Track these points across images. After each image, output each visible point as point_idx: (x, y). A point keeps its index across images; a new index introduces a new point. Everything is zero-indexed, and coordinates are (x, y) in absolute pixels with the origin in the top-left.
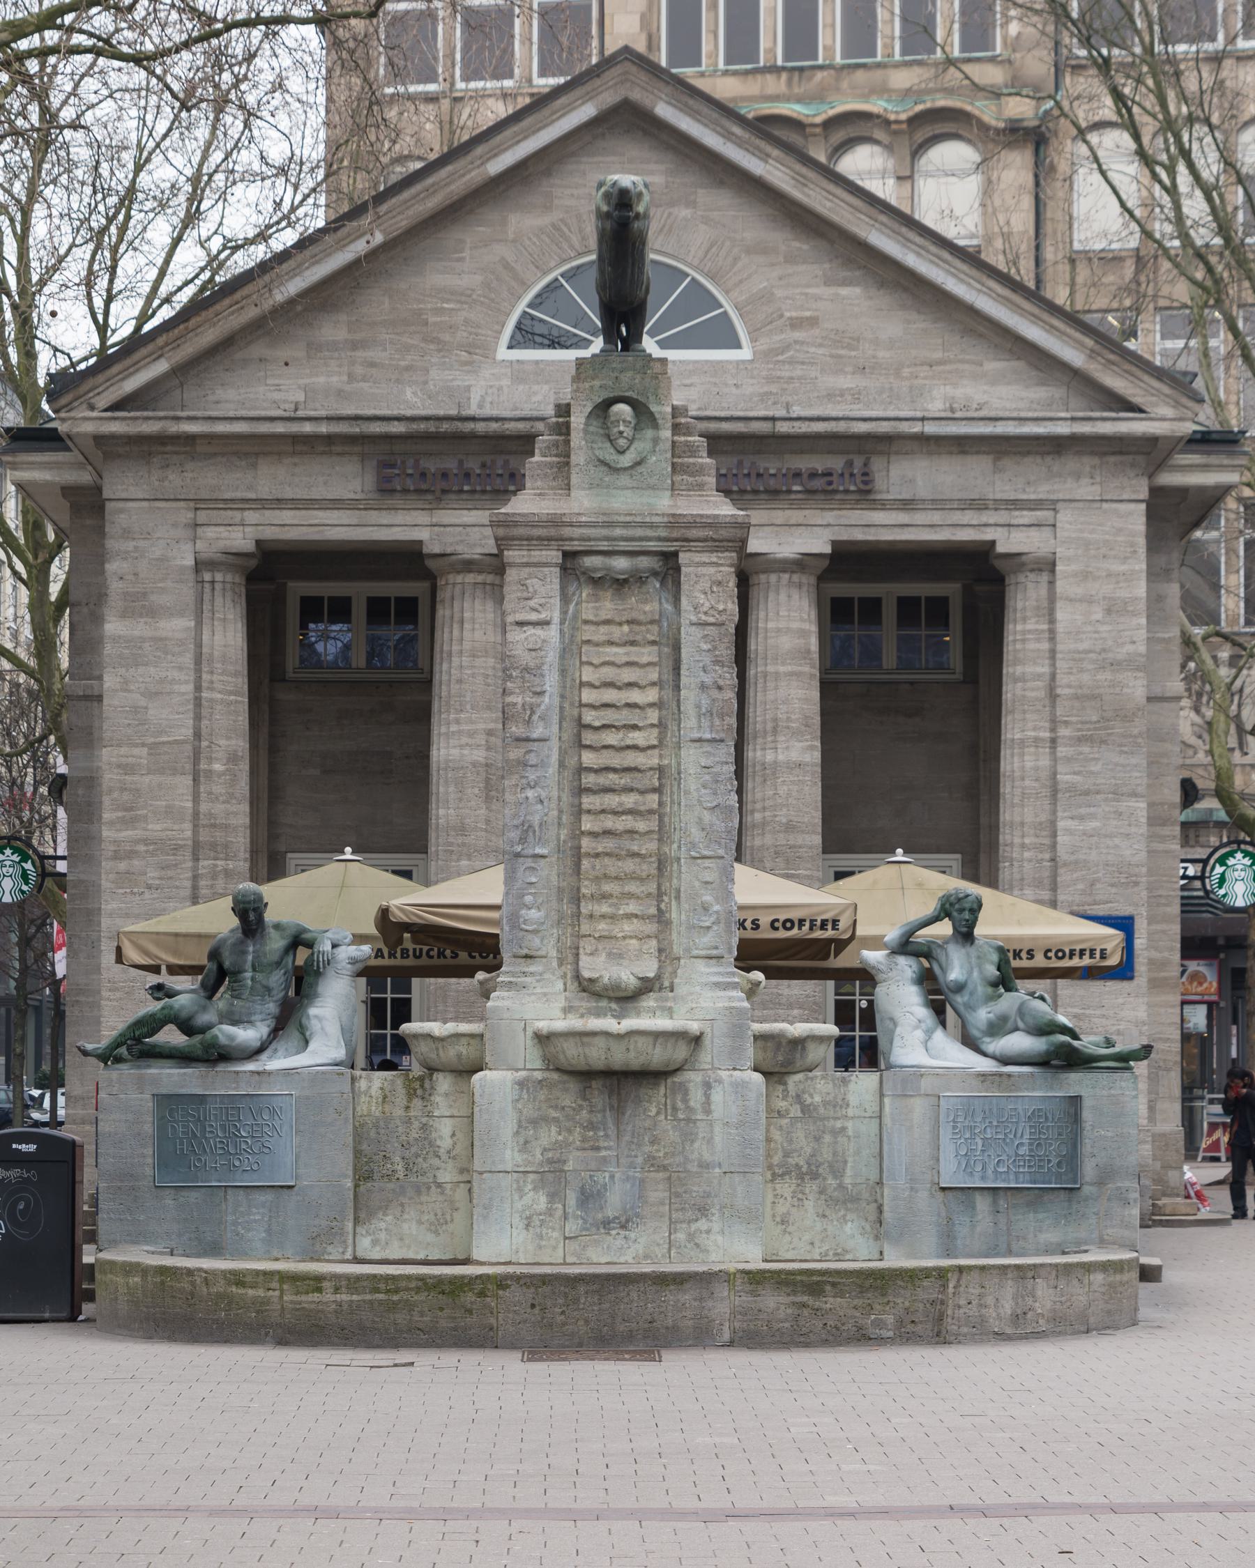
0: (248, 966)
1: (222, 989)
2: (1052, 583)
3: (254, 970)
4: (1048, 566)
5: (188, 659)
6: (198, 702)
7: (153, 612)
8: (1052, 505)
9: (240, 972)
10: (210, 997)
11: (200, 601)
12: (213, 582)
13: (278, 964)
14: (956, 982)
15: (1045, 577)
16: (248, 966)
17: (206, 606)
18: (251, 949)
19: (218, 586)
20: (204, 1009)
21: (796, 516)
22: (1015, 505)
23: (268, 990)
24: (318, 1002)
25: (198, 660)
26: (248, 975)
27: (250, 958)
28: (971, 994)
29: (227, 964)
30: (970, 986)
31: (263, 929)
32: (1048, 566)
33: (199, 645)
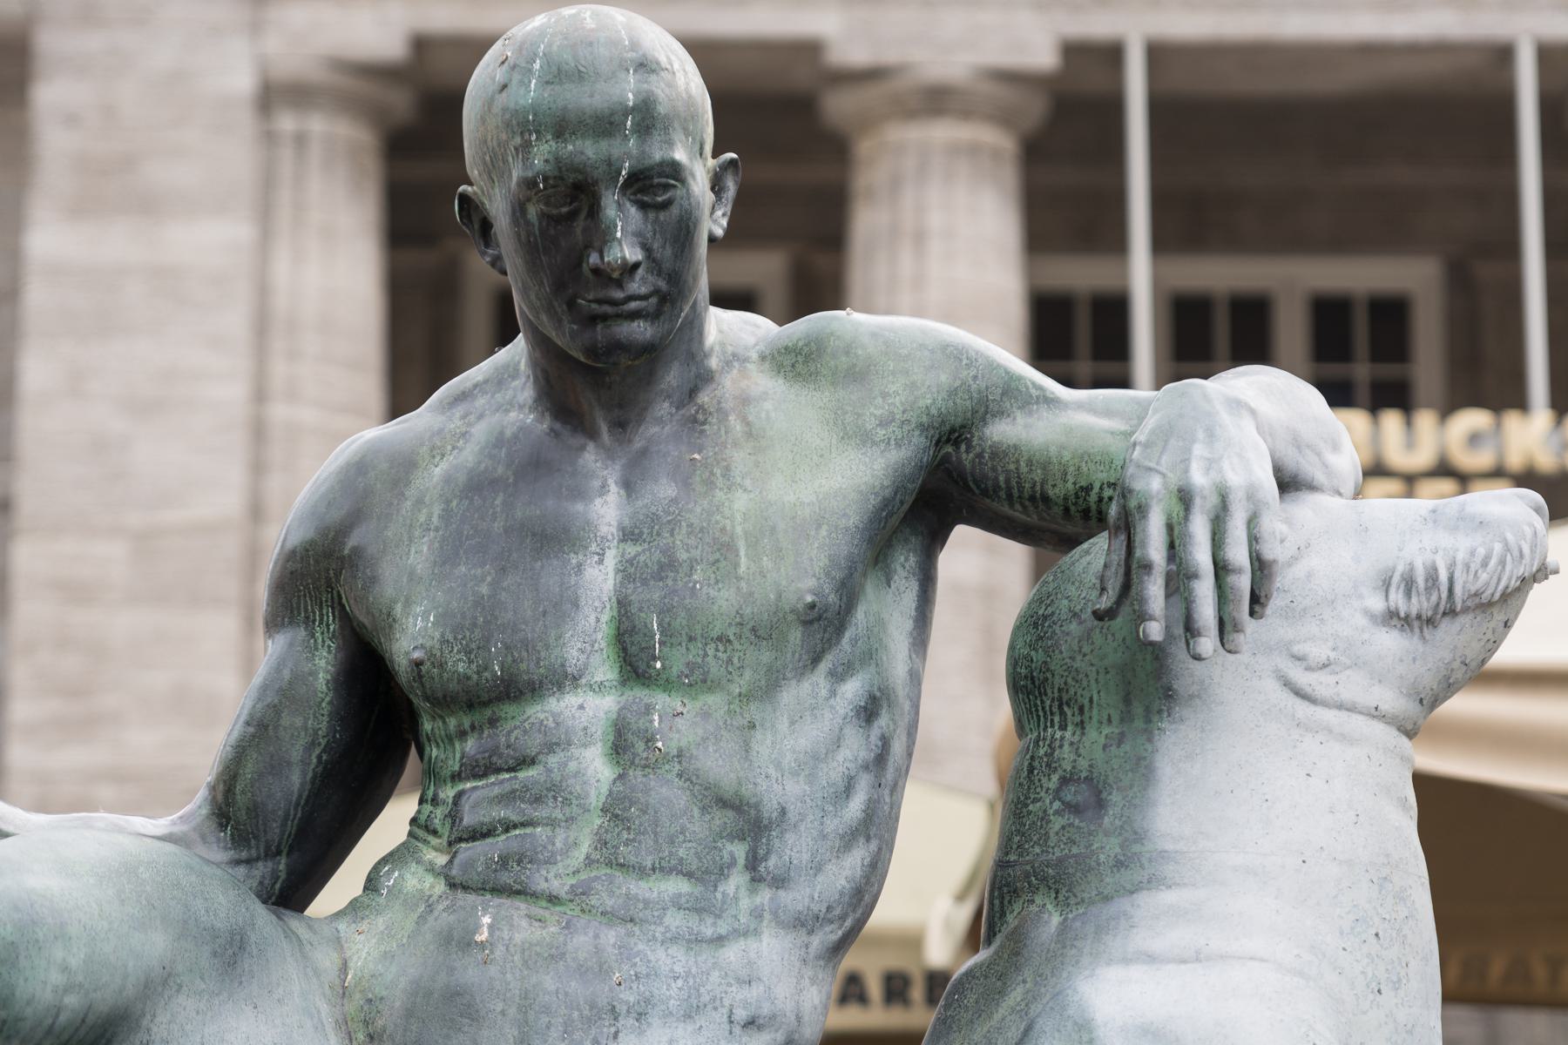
0: (586, 640)
1: (392, 823)
3: (635, 666)
5: (235, 321)
6: (259, 432)
7: (149, 207)
9: (515, 689)
10: (292, 893)
11: (267, 184)
12: (301, 140)
13: (824, 625)
16: (586, 640)
17: (285, 196)
18: (607, 510)
19: (315, 152)
20: (231, 956)
23: (751, 824)
24: (1156, 918)
25: (262, 325)
26: (588, 707)
27: (599, 578)
29: (413, 636)
31: (702, 378)
33: (263, 291)
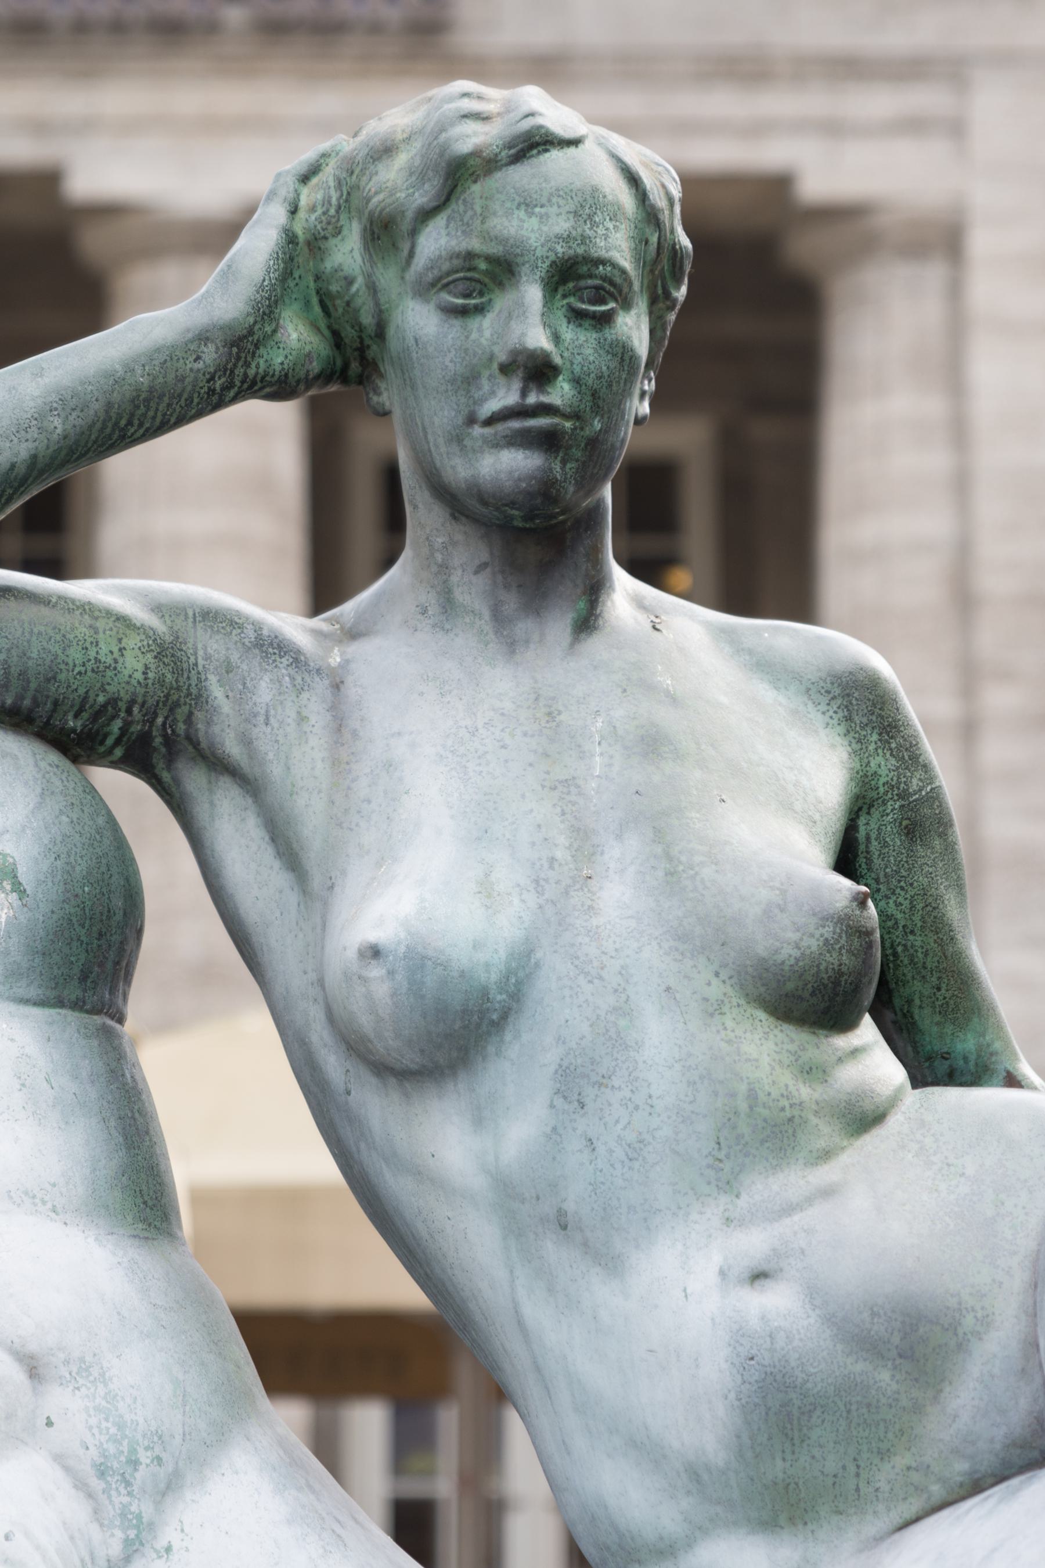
2: (955, 291)
4: (944, 240)
8: (950, 69)
14: (417, 962)
15: (933, 274)
21: (231, 97)
22: (848, 68)
28: (575, 1085)
30: (557, 1021)
32: (944, 240)
